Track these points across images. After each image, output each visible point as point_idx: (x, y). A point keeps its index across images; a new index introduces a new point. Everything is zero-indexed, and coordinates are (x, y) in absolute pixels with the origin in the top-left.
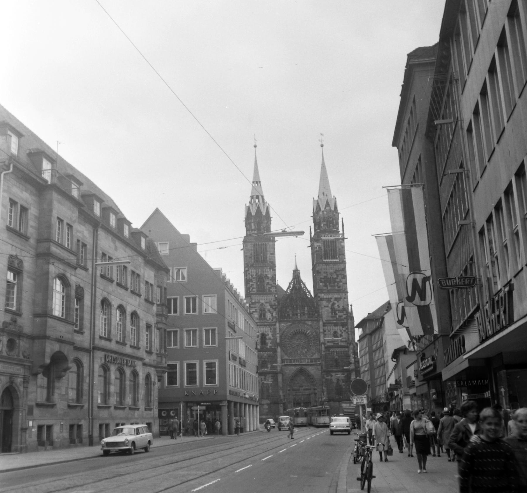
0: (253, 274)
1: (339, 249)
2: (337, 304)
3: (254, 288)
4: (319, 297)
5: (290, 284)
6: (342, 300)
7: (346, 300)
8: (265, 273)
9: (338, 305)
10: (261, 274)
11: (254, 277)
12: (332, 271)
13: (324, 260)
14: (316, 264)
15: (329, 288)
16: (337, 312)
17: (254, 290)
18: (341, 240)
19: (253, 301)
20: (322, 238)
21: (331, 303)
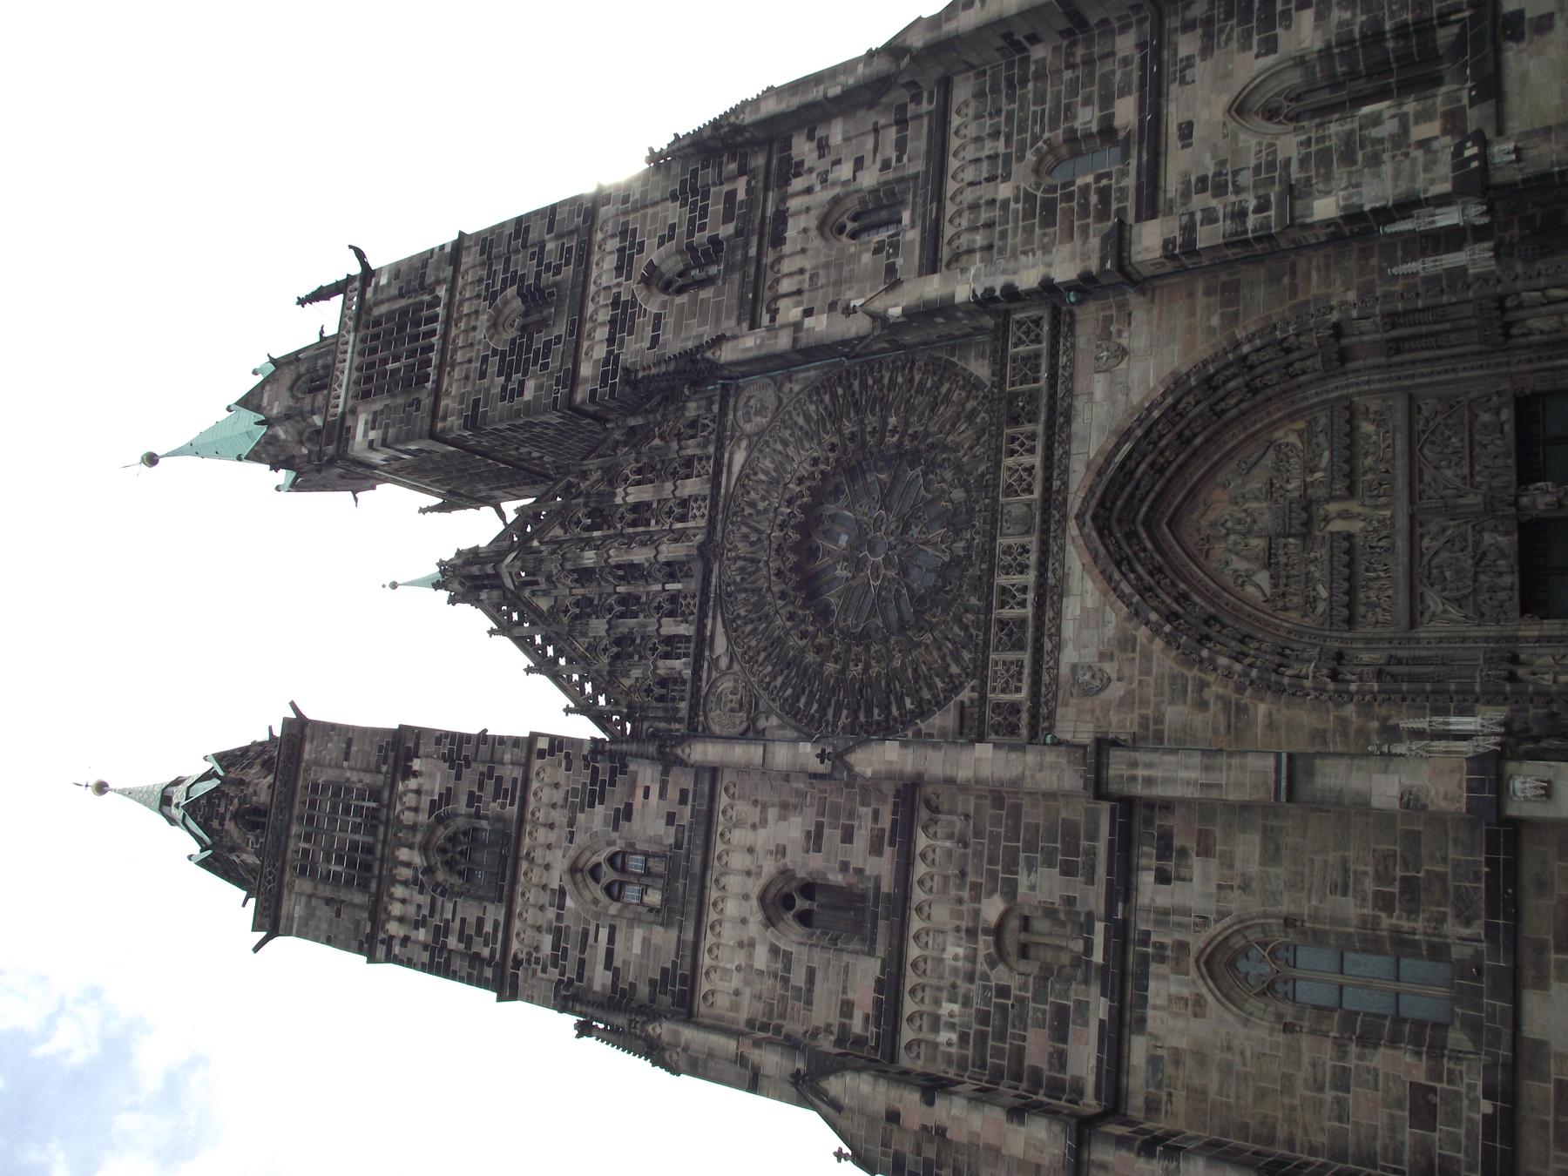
1: (401, 295)
2: (653, 254)
3: (480, 922)
4: (593, 392)
5: (504, 628)
8: (423, 817)
10: (424, 849)
11: (424, 900)
13: (429, 385)
14: (433, 435)
15: (561, 329)
16: (700, 238)
17: (488, 928)
19: (547, 941)
20: (340, 410)
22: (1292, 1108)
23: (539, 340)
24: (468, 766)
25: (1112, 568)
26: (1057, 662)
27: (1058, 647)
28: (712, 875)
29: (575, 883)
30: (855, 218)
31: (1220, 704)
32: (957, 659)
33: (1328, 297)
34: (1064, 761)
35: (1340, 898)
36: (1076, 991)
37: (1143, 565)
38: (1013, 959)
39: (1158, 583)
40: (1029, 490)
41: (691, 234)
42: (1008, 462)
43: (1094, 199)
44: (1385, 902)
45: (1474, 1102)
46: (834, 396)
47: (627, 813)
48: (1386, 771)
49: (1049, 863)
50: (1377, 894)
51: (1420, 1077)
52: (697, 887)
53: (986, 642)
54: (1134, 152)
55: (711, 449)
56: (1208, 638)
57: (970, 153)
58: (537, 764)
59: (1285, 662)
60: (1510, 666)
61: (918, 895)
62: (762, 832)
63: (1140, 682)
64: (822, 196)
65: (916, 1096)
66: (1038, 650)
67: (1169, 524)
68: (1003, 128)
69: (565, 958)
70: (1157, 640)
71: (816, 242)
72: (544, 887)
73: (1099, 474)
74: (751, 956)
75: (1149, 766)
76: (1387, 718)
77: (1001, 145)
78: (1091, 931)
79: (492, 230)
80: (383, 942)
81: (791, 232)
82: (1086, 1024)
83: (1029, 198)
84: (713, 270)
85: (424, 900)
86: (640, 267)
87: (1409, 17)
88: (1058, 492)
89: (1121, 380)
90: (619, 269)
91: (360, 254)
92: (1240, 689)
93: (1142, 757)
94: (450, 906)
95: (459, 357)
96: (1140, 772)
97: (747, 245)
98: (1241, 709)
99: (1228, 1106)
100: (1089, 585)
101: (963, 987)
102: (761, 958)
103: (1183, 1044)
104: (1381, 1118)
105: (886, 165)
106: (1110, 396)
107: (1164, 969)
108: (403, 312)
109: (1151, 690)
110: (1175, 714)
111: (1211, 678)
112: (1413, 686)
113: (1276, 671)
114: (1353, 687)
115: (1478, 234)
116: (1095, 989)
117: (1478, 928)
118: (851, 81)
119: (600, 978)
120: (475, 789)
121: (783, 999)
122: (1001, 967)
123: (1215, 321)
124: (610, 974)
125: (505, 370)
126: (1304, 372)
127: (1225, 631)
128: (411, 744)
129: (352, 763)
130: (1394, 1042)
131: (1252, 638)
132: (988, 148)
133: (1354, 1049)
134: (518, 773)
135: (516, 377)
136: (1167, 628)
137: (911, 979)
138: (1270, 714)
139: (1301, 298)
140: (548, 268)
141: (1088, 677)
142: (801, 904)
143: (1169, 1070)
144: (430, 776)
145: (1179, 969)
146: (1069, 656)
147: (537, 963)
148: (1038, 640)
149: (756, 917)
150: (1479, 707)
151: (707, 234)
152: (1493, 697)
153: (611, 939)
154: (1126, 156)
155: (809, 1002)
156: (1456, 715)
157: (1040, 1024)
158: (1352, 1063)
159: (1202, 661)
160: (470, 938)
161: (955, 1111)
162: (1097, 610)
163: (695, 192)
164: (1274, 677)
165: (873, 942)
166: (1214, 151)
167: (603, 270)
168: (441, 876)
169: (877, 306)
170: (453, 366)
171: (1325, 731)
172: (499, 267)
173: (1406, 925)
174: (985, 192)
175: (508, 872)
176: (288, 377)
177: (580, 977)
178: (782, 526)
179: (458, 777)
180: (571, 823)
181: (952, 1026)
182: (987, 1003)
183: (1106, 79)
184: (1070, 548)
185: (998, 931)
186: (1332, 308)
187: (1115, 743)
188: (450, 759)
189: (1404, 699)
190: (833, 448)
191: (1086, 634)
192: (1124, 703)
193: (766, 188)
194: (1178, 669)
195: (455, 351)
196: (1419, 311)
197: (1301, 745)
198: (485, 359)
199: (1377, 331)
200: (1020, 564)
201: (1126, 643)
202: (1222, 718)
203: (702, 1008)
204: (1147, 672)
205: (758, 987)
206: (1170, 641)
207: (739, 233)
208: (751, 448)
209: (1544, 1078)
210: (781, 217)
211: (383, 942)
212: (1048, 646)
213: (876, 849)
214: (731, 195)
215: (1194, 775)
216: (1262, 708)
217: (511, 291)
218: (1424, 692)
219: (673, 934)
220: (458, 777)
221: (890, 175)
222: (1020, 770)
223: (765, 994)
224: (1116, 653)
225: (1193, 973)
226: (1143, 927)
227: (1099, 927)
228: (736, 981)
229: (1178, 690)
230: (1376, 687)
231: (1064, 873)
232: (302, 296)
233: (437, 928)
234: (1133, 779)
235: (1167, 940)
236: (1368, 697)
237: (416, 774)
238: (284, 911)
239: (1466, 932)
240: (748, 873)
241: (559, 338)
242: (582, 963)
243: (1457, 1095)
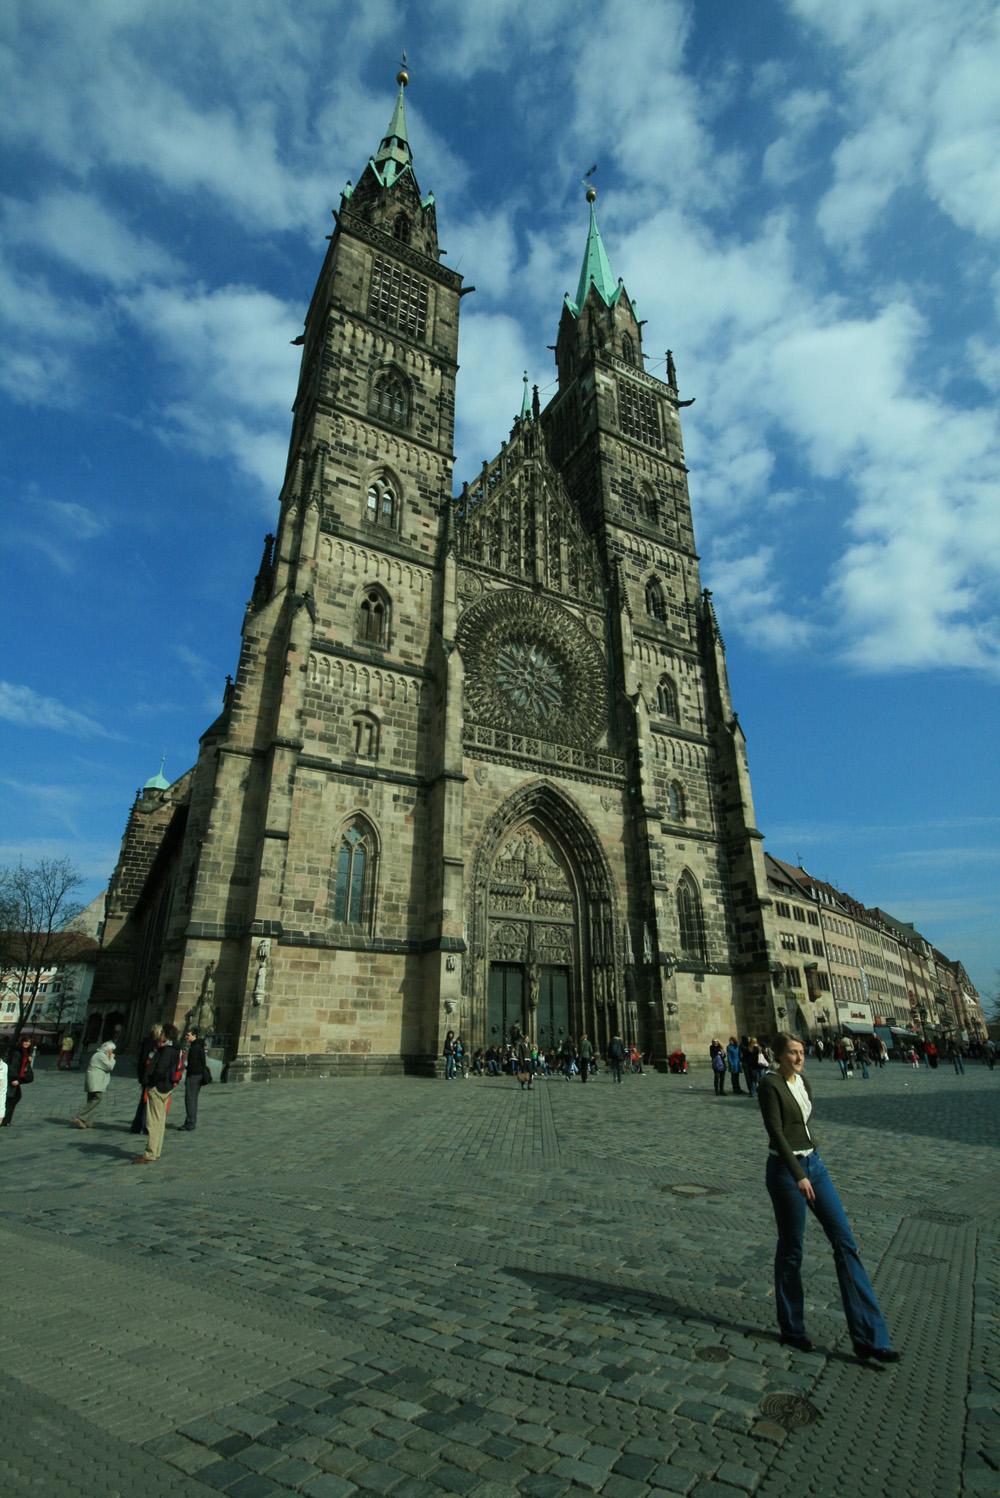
0: (360, 345)
1: (665, 424)
2: (665, 583)
3: (356, 396)
4: (610, 535)
6: (680, 574)
7: (692, 580)
9: (669, 589)
10: (393, 366)
11: (366, 358)
12: (646, 475)
13: (622, 433)
15: (639, 523)
17: (354, 401)
18: (668, 403)
19: (348, 440)
21: (649, 572)
22: (299, 847)
23: (635, 507)
24: (440, 410)
26: (488, 761)
27: (495, 762)
28: (389, 557)
29: (379, 468)
30: (665, 690)
32: (487, 711)
34: (456, 761)
35: (389, 877)
36: (343, 749)
38: (354, 718)
40: (559, 759)
41: (670, 605)
42: (571, 750)
43: (661, 804)
44: (388, 897)
45: (308, 928)
46: (596, 667)
47: (416, 511)
48: (457, 905)
49: (400, 743)
50: (391, 894)
51: (317, 906)
52: (381, 546)
54: (677, 824)
55: (580, 598)
57: (685, 752)
58: (440, 458)
61: (384, 673)
62: (409, 590)
64: (677, 677)
65: (304, 662)
68: (692, 768)
69: (341, 451)
71: (661, 670)
72: (377, 447)
73: (562, 792)
74: (349, 572)
77: (686, 765)
78: (371, 759)
79: (687, 491)
80: (342, 318)
81: (668, 660)
82: (329, 751)
83: (665, 776)
84: (653, 613)
85: (366, 358)
86: (661, 575)
87: (708, 940)
89: (600, 809)
90: (660, 562)
91: (688, 403)
92: (477, 844)
94: (363, 375)
95: (633, 455)
96: (454, 797)
97: (664, 635)
98: (469, 843)
99: (297, 818)
100: (519, 781)
101: (342, 690)
102: (349, 578)
103: (324, 799)
104: (298, 888)
105: (685, 711)
106: (591, 801)
107: (356, 794)
108: (656, 424)
109: (476, 803)
110: (468, 812)
111: (481, 831)
116: (345, 759)
117: (379, 935)
118: (724, 702)
119: (332, 473)
120: (426, 411)
121: (329, 587)
122: (352, 712)
123: (615, 851)
124: (334, 480)
125: (625, 484)
128: (449, 372)
129: (439, 324)
130: (330, 895)
132: (686, 760)
133: (327, 878)
134: (434, 444)
135: (620, 489)
137: (345, 663)
140: (666, 521)
142: (373, 604)
143: (312, 791)
144: (432, 380)
145: (357, 801)
146: (491, 766)
147: (338, 431)
148: (500, 754)
149: (371, 578)
151: (669, 614)
153: (352, 485)
154: (675, 821)
155: (328, 602)
157: (327, 728)
158: (321, 876)
160: (347, 386)
161: (298, 682)
163: (688, 611)
165: (360, 644)
166: (674, 858)
167: (661, 553)
168: (378, 373)
169: (641, 701)
170: (629, 451)
172: (669, 491)
173: (379, 905)
174: (670, 756)
175: (384, 423)
176: (633, 331)
177: (331, 459)
178: (545, 630)
179: (432, 401)
180: (410, 473)
181: (323, 681)
182: (336, 702)
183: (704, 816)
184: (535, 774)
185: (367, 713)
188: (441, 398)
190: (576, 663)
192: (472, 791)
193: (685, 650)
194: (485, 817)
195: (636, 454)
198: (630, 472)
201: (496, 795)
203: (323, 536)
205: (334, 573)
206: (496, 815)
207: (667, 631)
208: (579, 620)
209: (320, 958)
210: (671, 655)
211: (342, 318)
212: (497, 758)
213: (403, 654)
214: (682, 630)
215: (453, 821)
216: (469, 853)
217: (658, 496)
219: (357, 526)
220: (432, 401)
221: (681, 712)
223: (331, 577)
225: (356, 808)
226: (374, 785)
227: (372, 764)
228: (337, 561)
229: (477, 816)
231: (395, 750)
232: (673, 355)
233: (351, 363)
234: (451, 794)
235: (369, 797)
237: (432, 370)
238: (354, 241)
239: (378, 930)
240: (389, 579)
241: (635, 520)
242: (339, 462)
243: (310, 921)
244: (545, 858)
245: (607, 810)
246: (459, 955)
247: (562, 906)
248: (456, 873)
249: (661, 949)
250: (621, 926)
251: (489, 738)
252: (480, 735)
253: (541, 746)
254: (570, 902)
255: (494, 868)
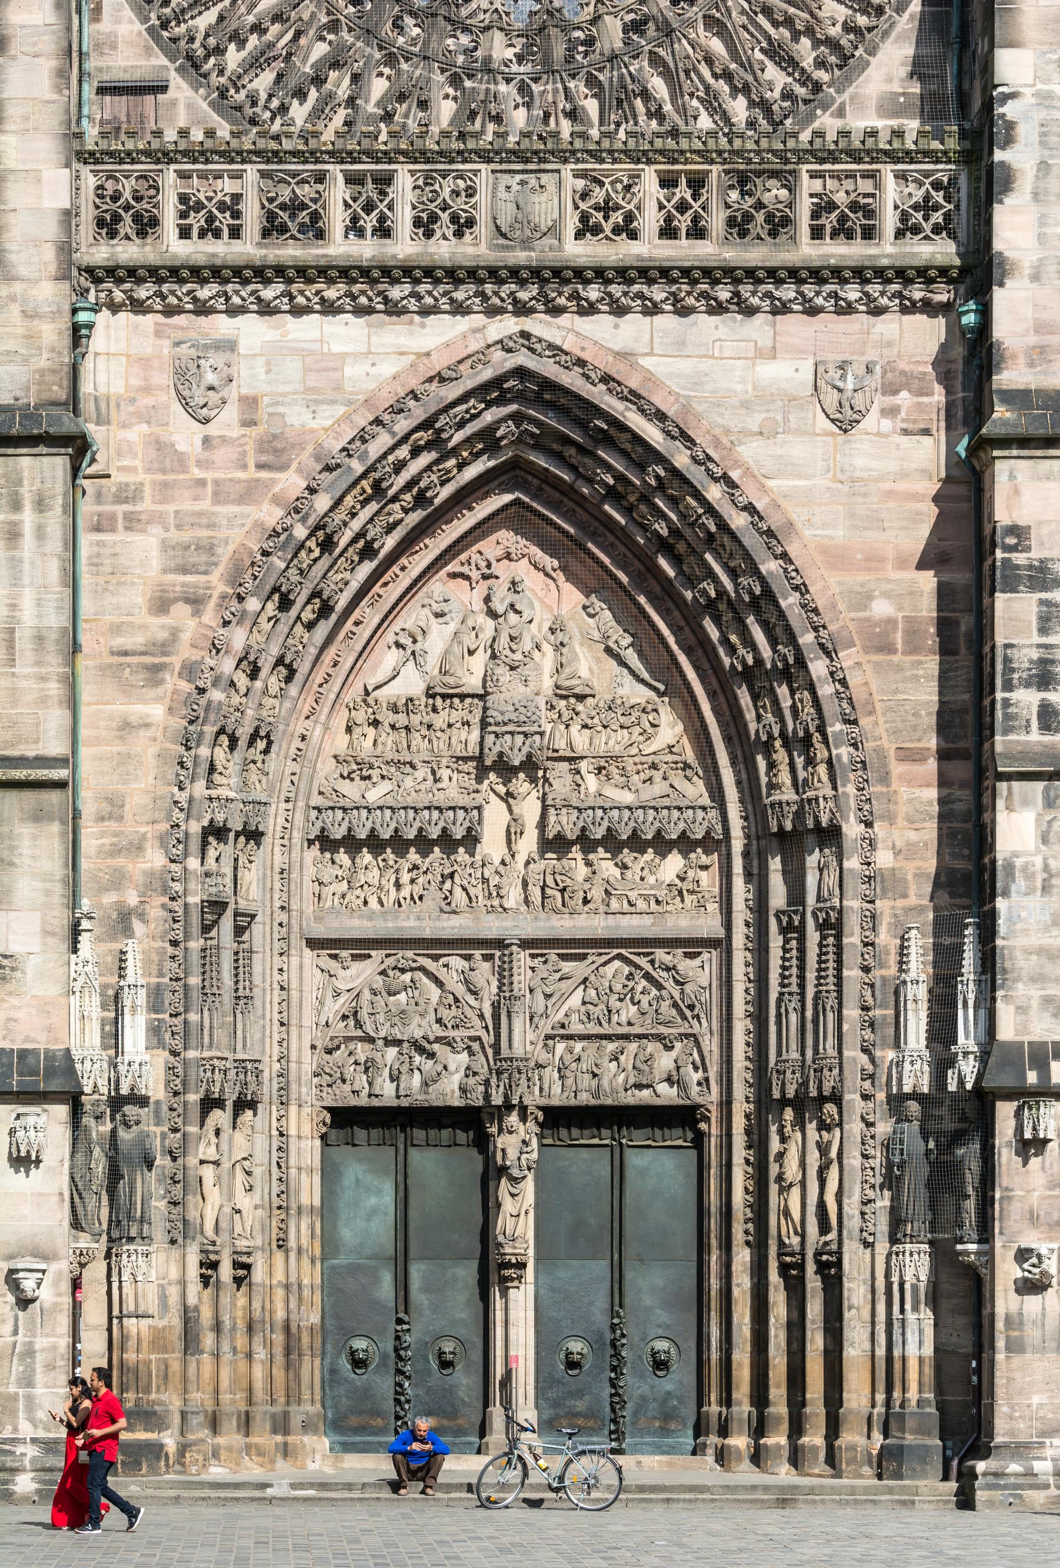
25: (419, 413)
26: (241, 310)
27: (267, 310)
31: (163, 635)
33: (890, 818)
37: (429, 468)
39: (395, 499)
48: (47, 933)
53: (276, 156)
56: (285, 604)
59: (242, 743)
60: (230, 1098)
63: (202, 483)
66: (261, 273)
67: (517, 502)
70: (280, 513)
75: (40, 533)
76: (142, 917)
88: (575, 296)
92: (190, 671)
93: (55, 521)
96: (28, 517)
100: (387, 369)
109: (188, 506)
111: (210, 616)
112: (195, 959)
113: (222, 731)
114: (193, 863)
115: (939, 1078)
126: (772, 765)
127: (299, 629)
131: (289, 679)
136: (300, 532)
138: (147, 725)
139: (897, 769)
141: (210, 378)
146: (251, 331)
148: (280, 271)
150: (162, 1057)
152: (178, 1082)
156: (149, 1022)
159: (241, 599)
162: (338, 388)
164: (210, 730)
171: (121, 818)
186: (869, 824)
187: (79, 448)
189: (174, 943)
191: (292, 367)
194: (225, 555)
196: (839, 969)
197: (93, 778)
199: (819, 899)
200: (434, 218)
201: (274, 453)
202: (134, 640)
204: (218, 497)
216: (157, 712)
218: (187, 974)
222: (23, 271)
224: (254, 432)
230: (194, 900)
236: (177, 887)
244: (589, 666)
245: (845, 426)
246: (61, 1111)
247: (674, 863)
248: (38, 816)
249: (1006, 1032)
250: (885, 938)
251: (233, 206)
252: (187, 205)
253: (491, 192)
254: (708, 843)
255: (340, 742)
